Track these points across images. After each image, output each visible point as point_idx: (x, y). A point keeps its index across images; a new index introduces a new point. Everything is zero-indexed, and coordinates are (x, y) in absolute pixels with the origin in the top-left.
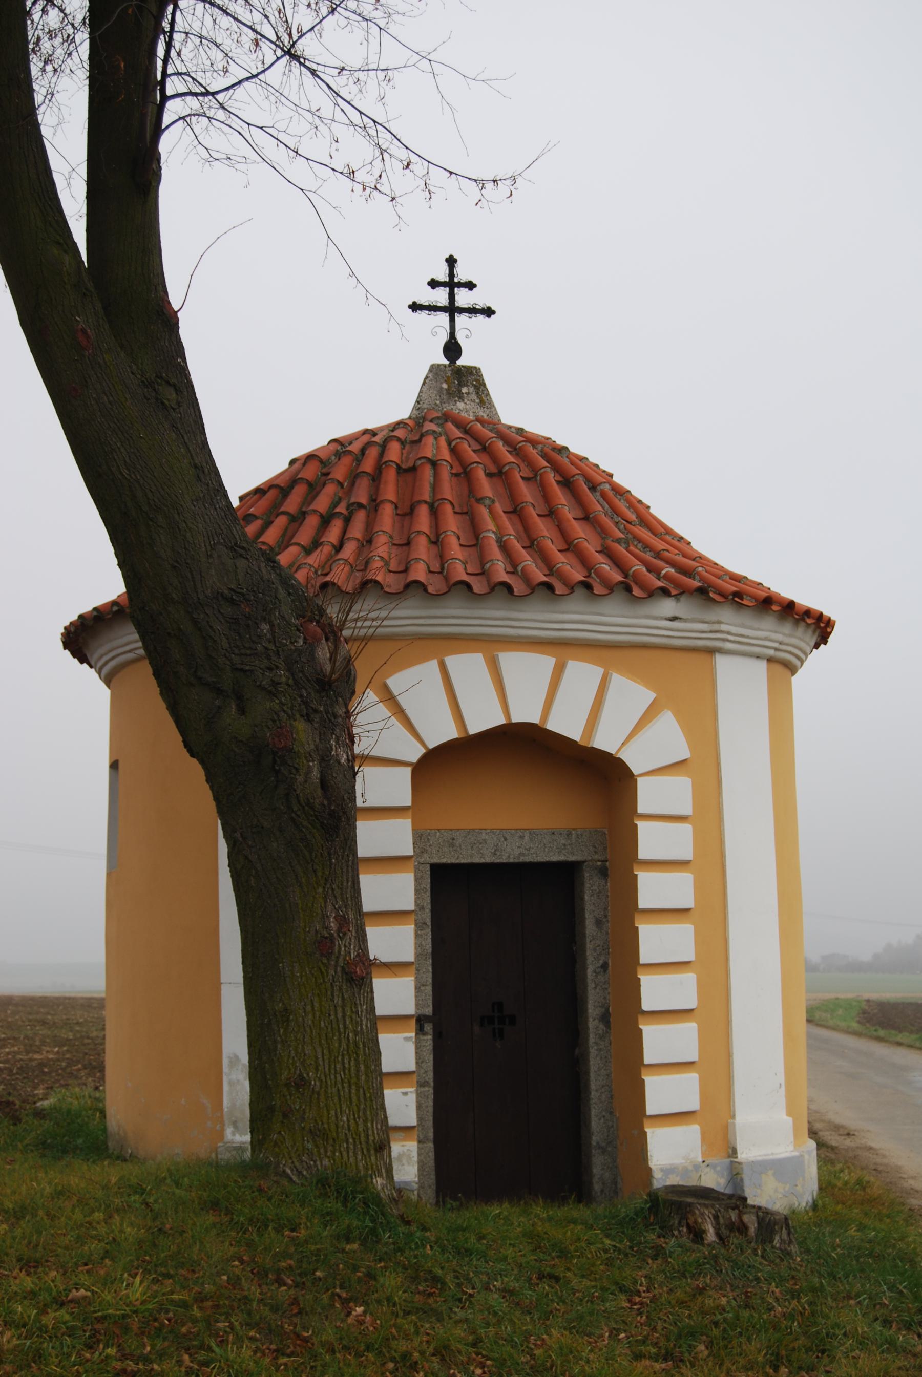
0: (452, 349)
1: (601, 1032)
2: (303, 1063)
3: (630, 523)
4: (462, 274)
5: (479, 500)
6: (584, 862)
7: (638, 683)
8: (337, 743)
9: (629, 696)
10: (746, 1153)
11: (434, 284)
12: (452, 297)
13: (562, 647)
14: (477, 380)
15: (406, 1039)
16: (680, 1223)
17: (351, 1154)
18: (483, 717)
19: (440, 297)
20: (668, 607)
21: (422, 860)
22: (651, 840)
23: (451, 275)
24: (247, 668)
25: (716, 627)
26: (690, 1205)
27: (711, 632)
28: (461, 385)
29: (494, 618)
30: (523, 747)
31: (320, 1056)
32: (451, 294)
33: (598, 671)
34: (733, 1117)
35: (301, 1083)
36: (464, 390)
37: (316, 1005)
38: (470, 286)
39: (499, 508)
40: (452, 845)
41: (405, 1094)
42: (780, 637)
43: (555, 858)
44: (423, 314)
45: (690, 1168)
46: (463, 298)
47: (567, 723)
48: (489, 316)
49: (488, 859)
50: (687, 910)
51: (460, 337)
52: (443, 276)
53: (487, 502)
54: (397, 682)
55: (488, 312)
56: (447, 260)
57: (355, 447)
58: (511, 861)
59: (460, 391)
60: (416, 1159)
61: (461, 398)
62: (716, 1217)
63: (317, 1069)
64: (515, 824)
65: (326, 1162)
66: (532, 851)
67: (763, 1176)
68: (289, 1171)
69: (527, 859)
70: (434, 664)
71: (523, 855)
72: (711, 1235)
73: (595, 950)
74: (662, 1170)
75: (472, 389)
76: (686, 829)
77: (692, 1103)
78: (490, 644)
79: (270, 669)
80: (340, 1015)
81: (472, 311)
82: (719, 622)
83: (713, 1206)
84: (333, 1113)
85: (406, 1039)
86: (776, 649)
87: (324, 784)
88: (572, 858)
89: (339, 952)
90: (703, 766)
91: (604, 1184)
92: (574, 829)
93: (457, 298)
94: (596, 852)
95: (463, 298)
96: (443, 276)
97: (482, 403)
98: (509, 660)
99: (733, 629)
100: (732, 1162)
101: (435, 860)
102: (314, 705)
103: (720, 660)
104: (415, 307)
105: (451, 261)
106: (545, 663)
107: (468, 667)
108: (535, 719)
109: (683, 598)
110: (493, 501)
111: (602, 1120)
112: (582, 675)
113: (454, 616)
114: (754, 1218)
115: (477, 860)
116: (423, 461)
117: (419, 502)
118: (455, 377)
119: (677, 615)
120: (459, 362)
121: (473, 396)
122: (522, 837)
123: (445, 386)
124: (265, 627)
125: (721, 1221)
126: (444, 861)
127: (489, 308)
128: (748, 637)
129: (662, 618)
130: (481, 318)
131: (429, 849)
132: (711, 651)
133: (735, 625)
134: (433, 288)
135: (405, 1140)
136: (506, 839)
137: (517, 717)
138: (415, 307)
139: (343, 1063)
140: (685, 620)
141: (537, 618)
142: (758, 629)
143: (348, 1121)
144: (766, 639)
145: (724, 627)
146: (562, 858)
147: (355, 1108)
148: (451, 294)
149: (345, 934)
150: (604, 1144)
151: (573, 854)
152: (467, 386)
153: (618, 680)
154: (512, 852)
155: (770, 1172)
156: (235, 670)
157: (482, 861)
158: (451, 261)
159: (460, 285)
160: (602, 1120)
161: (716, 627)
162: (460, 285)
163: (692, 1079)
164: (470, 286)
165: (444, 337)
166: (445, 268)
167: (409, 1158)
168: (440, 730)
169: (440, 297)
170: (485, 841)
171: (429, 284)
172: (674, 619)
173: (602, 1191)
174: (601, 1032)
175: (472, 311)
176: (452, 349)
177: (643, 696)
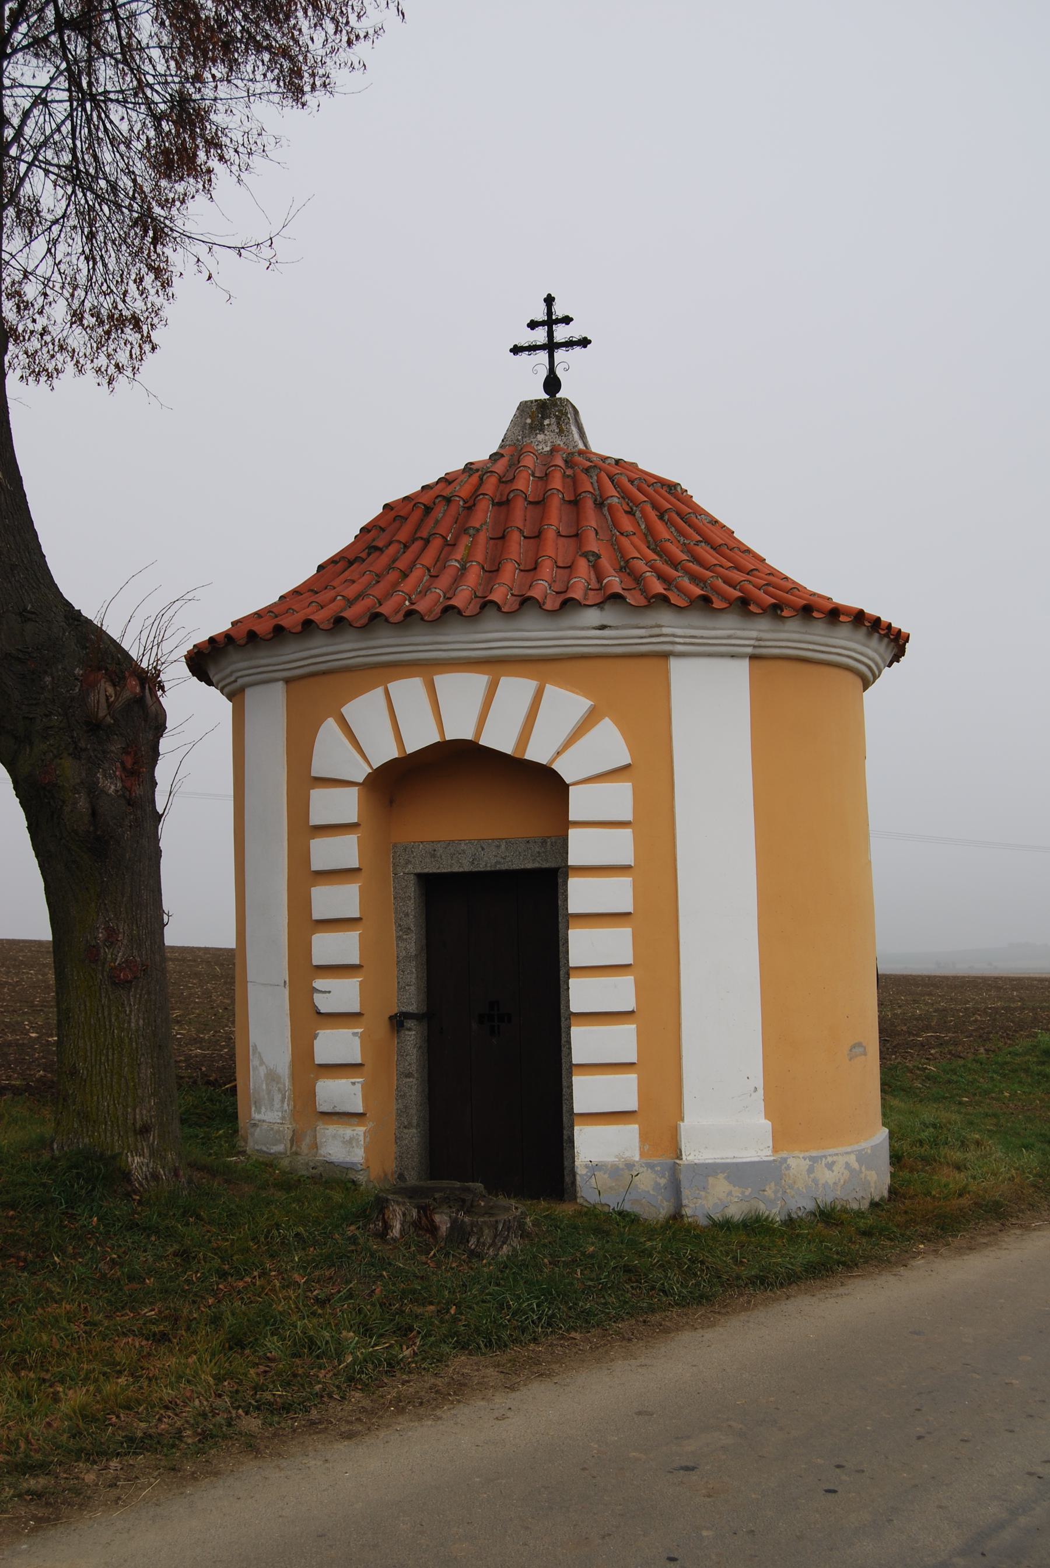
0: (552, 383)
2: (77, 1054)
3: (622, 534)
4: (559, 311)
5: (466, 531)
6: (558, 869)
7: (577, 693)
8: (104, 776)
9: (565, 705)
10: (693, 1153)
11: (533, 325)
12: (550, 334)
14: (560, 411)
15: (354, 1034)
17: (108, 1134)
18: (420, 736)
19: (540, 336)
20: (592, 617)
22: (581, 847)
23: (550, 313)
24: (31, 716)
26: (387, 1200)
28: (543, 418)
29: (420, 644)
30: (456, 765)
31: (88, 1048)
32: (551, 333)
34: (683, 1120)
35: (74, 1072)
36: (546, 422)
37: (88, 1004)
38: (567, 320)
39: (482, 537)
40: (433, 856)
41: (354, 1084)
42: (754, 634)
43: (530, 866)
44: (524, 355)
45: (621, 1166)
46: (561, 333)
47: (500, 738)
48: (585, 347)
49: (467, 868)
50: (628, 914)
51: (559, 372)
52: (541, 315)
53: (472, 532)
54: (351, 710)
55: (584, 342)
56: (545, 300)
57: (464, 490)
58: (489, 869)
59: (542, 424)
60: (362, 1143)
61: (542, 430)
62: (404, 1214)
63: (85, 1060)
64: (472, 835)
65: (87, 1140)
66: (508, 859)
67: (711, 1180)
68: (55, 1146)
69: (504, 867)
71: (500, 863)
74: (587, 1166)
75: (553, 420)
76: (628, 832)
77: (631, 1103)
78: (427, 668)
79: (46, 716)
80: (106, 1014)
81: (569, 344)
82: (660, 626)
83: (404, 1204)
84: (95, 1098)
85: (354, 1034)
86: (755, 647)
87: (94, 814)
88: (546, 865)
89: (105, 959)
90: (651, 770)
93: (555, 334)
95: (561, 333)
96: (541, 315)
97: (561, 431)
98: (444, 682)
101: (419, 871)
102: (82, 744)
103: (674, 664)
104: (516, 350)
105: (549, 300)
106: (477, 682)
107: (408, 691)
108: (468, 735)
109: (607, 606)
110: (478, 530)
112: (516, 691)
113: (387, 645)
114: (446, 1218)
116: (439, 499)
117: (417, 539)
118: (549, 410)
119: (605, 623)
120: (558, 396)
121: (554, 427)
122: (498, 847)
123: (529, 421)
124: (48, 679)
125: (408, 1218)
126: (426, 871)
127: (585, 339)
128: (702, 637)
129: (588, 628)
130: (578, 349)
132: (666, 656)
133: (681, 627)
134: (532, 329)
135: (358, 1125)
136: (483, 849)
138: (516, 350)
139: (107, 1056)
140: (616, 628)
141: (458, 640)
142: (714, 629)
143: (108, 1106)
144: (729, 637)
145: (665, 630)
146: (536, 865)
147: (116, 1095)
148: (551, 333)
149: (112, 943)
151: (547, 861)
152: (550, 417)
153: (551, 691)
154: (489, 861)
155: (721, 1176)
156: (24, 718)
157: (461, 870)
158: (549, 300)
159: (558, 321)
162: (558, 321)
164: (567, 320)
165: (544, 373)
166: (543, 307)
167: (358, 1141)
169: (540, 336)
170: (464, 852)
171: (529, 325)
172: (603, 627)
175: (569, 344)
176: (552, 383)
177: (578, 704)
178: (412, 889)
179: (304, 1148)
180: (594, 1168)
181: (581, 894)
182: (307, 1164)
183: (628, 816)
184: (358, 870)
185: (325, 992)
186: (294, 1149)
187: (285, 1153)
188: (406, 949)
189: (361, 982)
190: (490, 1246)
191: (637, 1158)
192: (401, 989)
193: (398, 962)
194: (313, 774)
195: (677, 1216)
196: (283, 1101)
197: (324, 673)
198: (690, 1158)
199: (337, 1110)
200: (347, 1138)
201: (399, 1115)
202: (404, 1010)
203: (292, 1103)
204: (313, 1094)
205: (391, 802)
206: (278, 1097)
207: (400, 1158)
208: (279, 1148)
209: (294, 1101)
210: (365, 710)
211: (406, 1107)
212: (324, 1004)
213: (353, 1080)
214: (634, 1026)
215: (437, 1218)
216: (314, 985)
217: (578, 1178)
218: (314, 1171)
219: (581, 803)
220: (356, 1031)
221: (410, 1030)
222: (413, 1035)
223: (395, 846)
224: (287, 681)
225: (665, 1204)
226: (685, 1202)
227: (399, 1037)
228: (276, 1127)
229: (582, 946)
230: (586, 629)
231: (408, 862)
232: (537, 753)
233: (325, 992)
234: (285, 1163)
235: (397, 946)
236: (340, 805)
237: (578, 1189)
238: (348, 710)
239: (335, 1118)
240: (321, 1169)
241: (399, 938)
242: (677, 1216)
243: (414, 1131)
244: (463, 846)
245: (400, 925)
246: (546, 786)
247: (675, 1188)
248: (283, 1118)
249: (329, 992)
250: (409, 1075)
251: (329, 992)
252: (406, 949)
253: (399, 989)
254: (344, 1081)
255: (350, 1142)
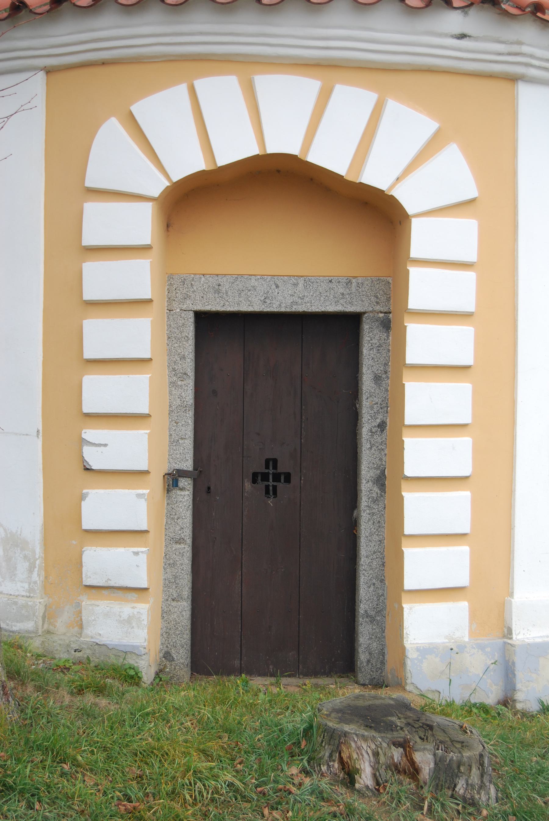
1: (374, 495)
6: (365, 313)
9: (407, 125)
10: (524, 633)
13: (329, 68)
15: (139, 496)
16: (331, 756)
18: (234, 146)
21: (184, 307)
22: (423, 288)
25: (515, 48)
26: (346, 734)
27: (509, 54)
30: (278, 181)
33: (371, 97)
34: (511, 594)
40: (218, 291)
41: (136, 554)
43: (331, 308)
47: (331, 155)
50: (467, 368)
54: (142, 109)
58: (283, 310)
60: (145, 622)
62: (376, 754)
66: (306, 300)
70: (182, 89)
72: (365, 778)
73: (372, 408)
74: (418, 649)
76: (470, 276)
77: (462, 578)
82: (520, 43)
83: (373, 739)
85: (139, 496)
91: (370, 654)
92: (355, 277)
94: (377, 303)
98: (267, 84)
99: (538, 52)
100: (505, 643)
101: (200, 307)
103: (523, 89)
106: (309, 87)
107: (220, 92)
109: (472, 11)
111: (372, 588)
112: (352, 102)
114: (430, 757)
115: (245, 308)
122: (296, 285)
125: (382, 759)
129: (446, 35)
131: (193, 295)
132: (513, 79)
135: (138, 601)
136: (277, 287)
137: (274, 147)
145: (525, 49)
150: (373, 613)
151: (351, 303)
153: (394, 108)
154: (282, 302)
157: (250, 309)
160: (372, 588)
161: (515, 48)
163: (462, 553)
168: (187, 161)
172: (462, 36)
173: (369, 661)
174: (374, 495)
177: (424, 126)
178: (190, 330)
179: (61, 625)
180: (426, 651)
181: (421, 343)
182: (68, 646)
183: (472, 256)
184: (150, 301)
185: (100, 445)
186: (46, 626)
187: (36, 632)
188: (180, 397)
189: (149, 435)
190: (481, 787)
191: (466, 639)
192: (174, 442)
193: (170, 412)
194: (88, 184)
195: (507, 702)
196: (31, 570)
197: (104, 63)
198: (520, 637)
199: (112, 584)
200: (125, 616)
201: (165, 585)
202: (177, 467)
203: (43, 573)
204: (80, 564)
205: (168, 226)
206: (22, 567)
207: (167, 634)
208: (29, 625)
209: (46, 571)
210: (163, 110)
211: (175, 577)
212: (95, 459)
213: (136, 549)
214: (468, 494)
215: (418, 757)
216: (84, 436)
217: (409, 663)
218: (78, 654)
219: (422, 238)
220: (140, 491)
221: (182, 489)
222: (185, 495)
223: (171, 277)
224: (49, 71)
225: (494, 687)
226: (519, 686)
227: (169, 498)
228: (21, 601)
229: (421, 401)
230: (447, 34)
231: (186, 297)
232: (376, 175)
233: (100, 445)
234: (35, 645)
235: (170, 393)
236: (139, 224)
237: (408, 675)
238: (142, 109)
239: (105, 592)
240: (88, 652)
241: (173, 384)
242: (507, 702)
243: (185, 603)
244: (253, 282)
245: (174, 370)
246: (378, 216)
247: (508, 672)
248: (31, 590)
249: (105, 445)
250: (179, 541)
251: (105, 445)
252: (180, 397)
253: (171, 443)
254: (121, 550)
255: (129, 621)
